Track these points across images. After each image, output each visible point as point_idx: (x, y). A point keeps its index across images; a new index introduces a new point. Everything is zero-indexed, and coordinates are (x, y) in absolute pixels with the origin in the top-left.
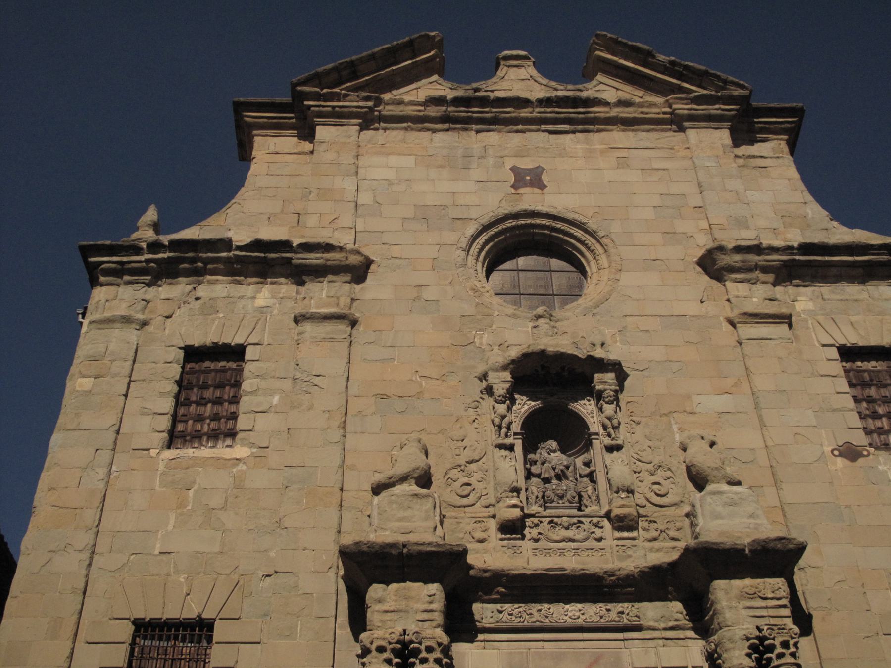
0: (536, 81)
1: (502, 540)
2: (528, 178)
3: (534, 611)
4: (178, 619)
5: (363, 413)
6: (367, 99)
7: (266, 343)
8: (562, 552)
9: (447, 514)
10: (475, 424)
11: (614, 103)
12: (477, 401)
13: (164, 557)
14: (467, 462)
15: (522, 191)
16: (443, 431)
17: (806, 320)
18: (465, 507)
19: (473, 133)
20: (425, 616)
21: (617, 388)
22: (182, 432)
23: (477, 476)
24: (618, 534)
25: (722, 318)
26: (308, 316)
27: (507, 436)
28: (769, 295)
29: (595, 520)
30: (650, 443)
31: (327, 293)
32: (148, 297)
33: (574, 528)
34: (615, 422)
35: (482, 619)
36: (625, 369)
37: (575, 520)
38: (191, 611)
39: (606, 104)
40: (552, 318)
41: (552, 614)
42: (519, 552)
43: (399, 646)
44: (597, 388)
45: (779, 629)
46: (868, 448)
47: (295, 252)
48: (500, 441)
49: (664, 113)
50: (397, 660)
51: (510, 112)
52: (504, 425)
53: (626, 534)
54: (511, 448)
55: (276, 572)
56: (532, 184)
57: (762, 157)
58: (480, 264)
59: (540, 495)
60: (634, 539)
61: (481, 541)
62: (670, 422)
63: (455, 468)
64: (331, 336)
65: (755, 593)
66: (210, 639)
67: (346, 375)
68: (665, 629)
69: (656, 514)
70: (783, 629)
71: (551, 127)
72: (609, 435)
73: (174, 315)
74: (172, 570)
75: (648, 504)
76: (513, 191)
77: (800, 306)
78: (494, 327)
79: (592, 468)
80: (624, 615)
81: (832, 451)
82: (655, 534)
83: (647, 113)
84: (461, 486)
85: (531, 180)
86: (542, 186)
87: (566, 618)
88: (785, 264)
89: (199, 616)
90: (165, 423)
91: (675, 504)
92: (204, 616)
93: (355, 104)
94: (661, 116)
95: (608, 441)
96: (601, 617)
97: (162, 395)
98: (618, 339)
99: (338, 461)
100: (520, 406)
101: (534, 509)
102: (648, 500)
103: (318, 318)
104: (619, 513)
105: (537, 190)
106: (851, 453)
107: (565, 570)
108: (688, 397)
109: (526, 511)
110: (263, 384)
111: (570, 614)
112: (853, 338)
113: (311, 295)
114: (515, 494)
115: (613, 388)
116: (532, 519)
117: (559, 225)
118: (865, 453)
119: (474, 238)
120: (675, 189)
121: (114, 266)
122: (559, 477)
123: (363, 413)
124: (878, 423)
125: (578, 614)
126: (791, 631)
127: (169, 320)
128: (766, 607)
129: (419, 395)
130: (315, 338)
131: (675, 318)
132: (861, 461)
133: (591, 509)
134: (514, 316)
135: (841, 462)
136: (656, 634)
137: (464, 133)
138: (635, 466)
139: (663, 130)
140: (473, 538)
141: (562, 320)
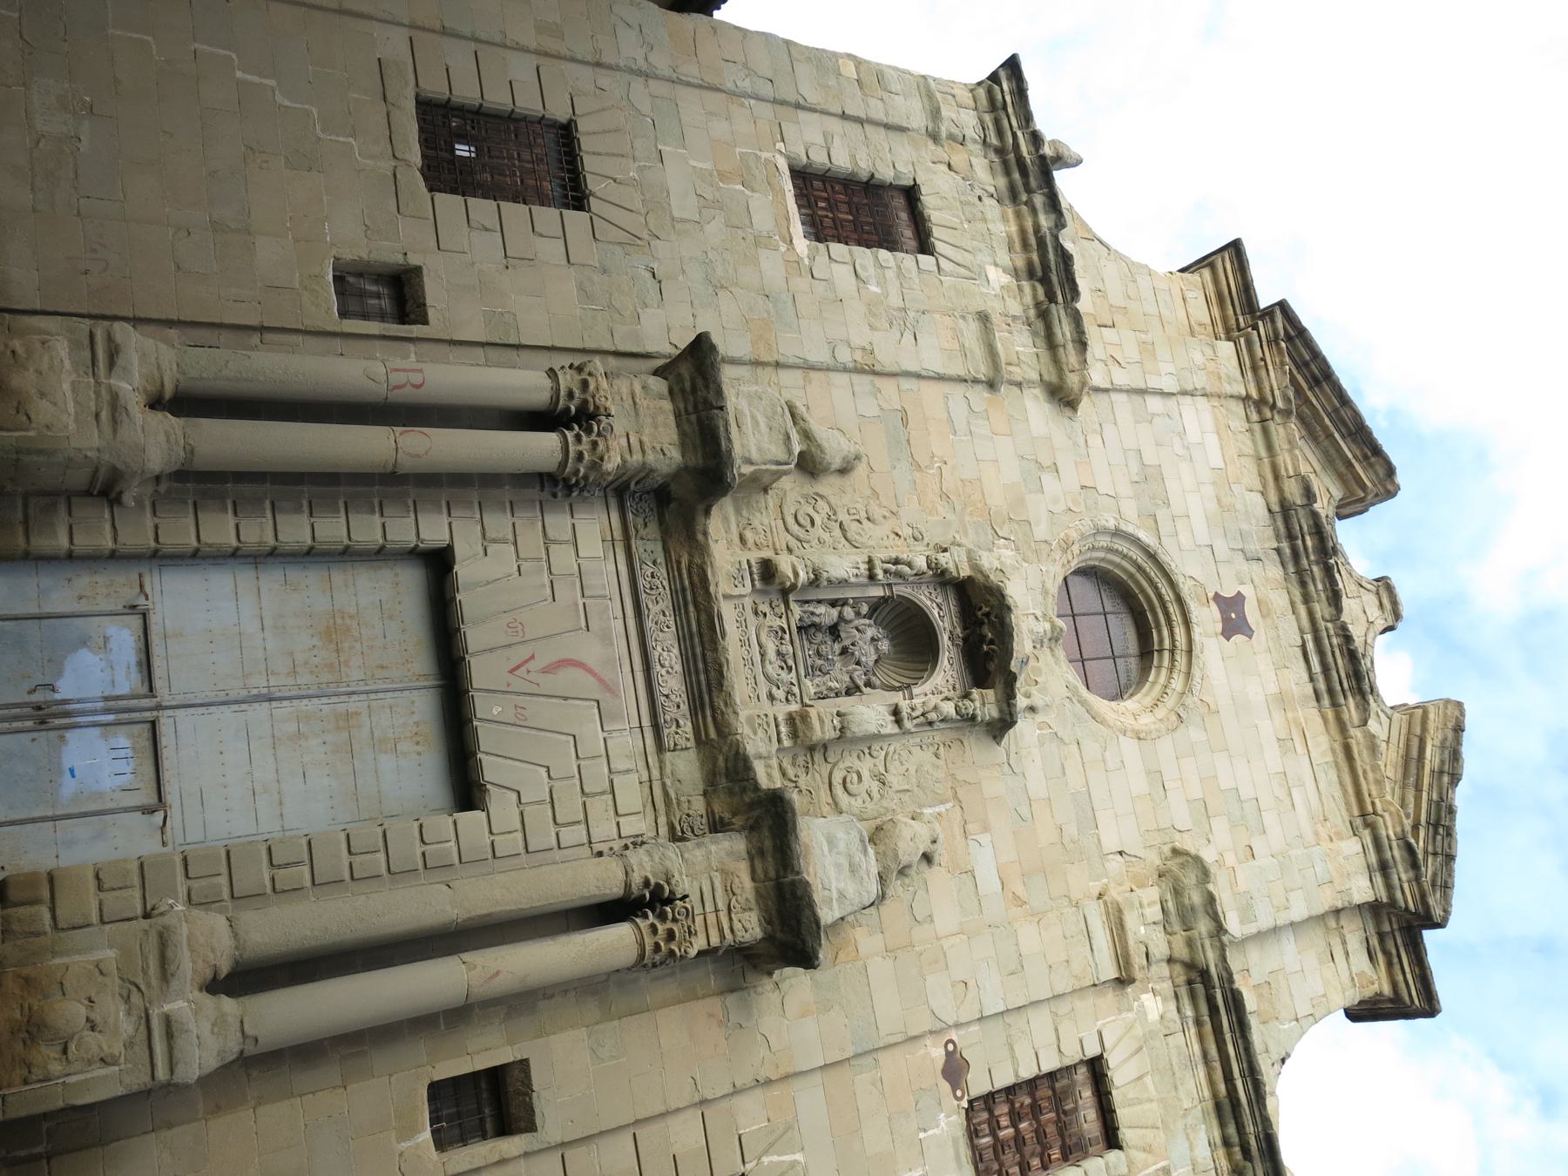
0: (1368, 629)
2: (1233, 616)
3: (662, 605)
4: (583, 169)
5: (879, 395)
6: (1286, 399)
7: (943, 278)
8: (747, 643)
9: (769, 497)
10: (892, 536)
11: (1369, 732)
13: (655, 155)
14: (841, 524)
15: (1214, 607)
16: (875, 494)
17: (1130, 1009)
18: (783, 519)
19: (1275, 545)
21: (979, 719)
23: (825, 536)
24: (781, 718)
25: (1105, 881)
26: (988, 325)
27: (886, 571)
29: (796, 690)
30: (912, 771)
32: (968, 142)
33: (779, 663)
34: (933, 716)
35: (642, 539)
36: (1006, 736)
37: (791, 662)
38: (593, 184)
39: (1364, 723)
40: (1053, 641)
41: (662, 631)
42: (737, 583)
43: (592, 408)
44: (973, 690)
45: (689, 927)
46: (966, 1098)
48: (878, 563)
49: (1373, 804)
50: (573, 408)
51: (1318, 587)
52: (899, 567)
53: (783, 729)
54: (872, 577)
55: (660, 282)
56: (1226, 620)
57: (1347, 954)
58: (1101, 554)
59: (817, 620)
60: (779, 741)
61: (742, 539)
62: (947, 801)
63: (831, 507)
64: (968, 355)
65: (734, 894)
66: (567, 206)
67: (924, 373)
68: (664, 785)
69: (817, 776)
70: (690, 933)
71: (1310, 646)
72: (913, 709)
74: (642, 164)
75: (829, 766)
76: (1211, 595)
77: (1147, 999)
78: (1025, 565)
79: (864, 689)
80: (674, 727)
81: (951, 1041)
82: (791, 772)
83: (1365, 778)
87: (659, 649)
88: (1204, 974)
89: (591, 194)
90: (819, 158)
91: (836, 804)
92: (591, 199)
94: (1368, 800)
95: (904, 705)
96: (667, 696)
97: (853, 157)
98: (1044, 732)
99: (813, 358)
100: (928, 594)
101: (797, 610)
102: (835, 765)
103: (988, 338)
104: (811, 715)
105: (1219, 627)
106: (954, 1069)
107: (723, 638)
108: (986, 829)
109: (791, 597)
110: (890, 274)
112: (1120, 1075)
113: (1015, 333)
114: (812, 576)
115: (978, 712)
116: (782, 606)
117: (1181, 659)
118: (959, 1093)
119: (1135, 541)
120: (1269, 819)
121: (999, 97)
122: (844, 651)
123: (879, 395)
124: (1004, 1121)
125: (667, 663)
126: (688, 944)
128: (717, 911)
130: (962, 335)
131: (1090, 813)
132: (945, 1086)
133: (810, 687)
134: (1045, 592)
135: (938, 1054)
136: (656, 773)
137: (1270, 532)
138: (878, 748)
139: (1347, 804)
140: (744, 529)
141: (1053, 655)
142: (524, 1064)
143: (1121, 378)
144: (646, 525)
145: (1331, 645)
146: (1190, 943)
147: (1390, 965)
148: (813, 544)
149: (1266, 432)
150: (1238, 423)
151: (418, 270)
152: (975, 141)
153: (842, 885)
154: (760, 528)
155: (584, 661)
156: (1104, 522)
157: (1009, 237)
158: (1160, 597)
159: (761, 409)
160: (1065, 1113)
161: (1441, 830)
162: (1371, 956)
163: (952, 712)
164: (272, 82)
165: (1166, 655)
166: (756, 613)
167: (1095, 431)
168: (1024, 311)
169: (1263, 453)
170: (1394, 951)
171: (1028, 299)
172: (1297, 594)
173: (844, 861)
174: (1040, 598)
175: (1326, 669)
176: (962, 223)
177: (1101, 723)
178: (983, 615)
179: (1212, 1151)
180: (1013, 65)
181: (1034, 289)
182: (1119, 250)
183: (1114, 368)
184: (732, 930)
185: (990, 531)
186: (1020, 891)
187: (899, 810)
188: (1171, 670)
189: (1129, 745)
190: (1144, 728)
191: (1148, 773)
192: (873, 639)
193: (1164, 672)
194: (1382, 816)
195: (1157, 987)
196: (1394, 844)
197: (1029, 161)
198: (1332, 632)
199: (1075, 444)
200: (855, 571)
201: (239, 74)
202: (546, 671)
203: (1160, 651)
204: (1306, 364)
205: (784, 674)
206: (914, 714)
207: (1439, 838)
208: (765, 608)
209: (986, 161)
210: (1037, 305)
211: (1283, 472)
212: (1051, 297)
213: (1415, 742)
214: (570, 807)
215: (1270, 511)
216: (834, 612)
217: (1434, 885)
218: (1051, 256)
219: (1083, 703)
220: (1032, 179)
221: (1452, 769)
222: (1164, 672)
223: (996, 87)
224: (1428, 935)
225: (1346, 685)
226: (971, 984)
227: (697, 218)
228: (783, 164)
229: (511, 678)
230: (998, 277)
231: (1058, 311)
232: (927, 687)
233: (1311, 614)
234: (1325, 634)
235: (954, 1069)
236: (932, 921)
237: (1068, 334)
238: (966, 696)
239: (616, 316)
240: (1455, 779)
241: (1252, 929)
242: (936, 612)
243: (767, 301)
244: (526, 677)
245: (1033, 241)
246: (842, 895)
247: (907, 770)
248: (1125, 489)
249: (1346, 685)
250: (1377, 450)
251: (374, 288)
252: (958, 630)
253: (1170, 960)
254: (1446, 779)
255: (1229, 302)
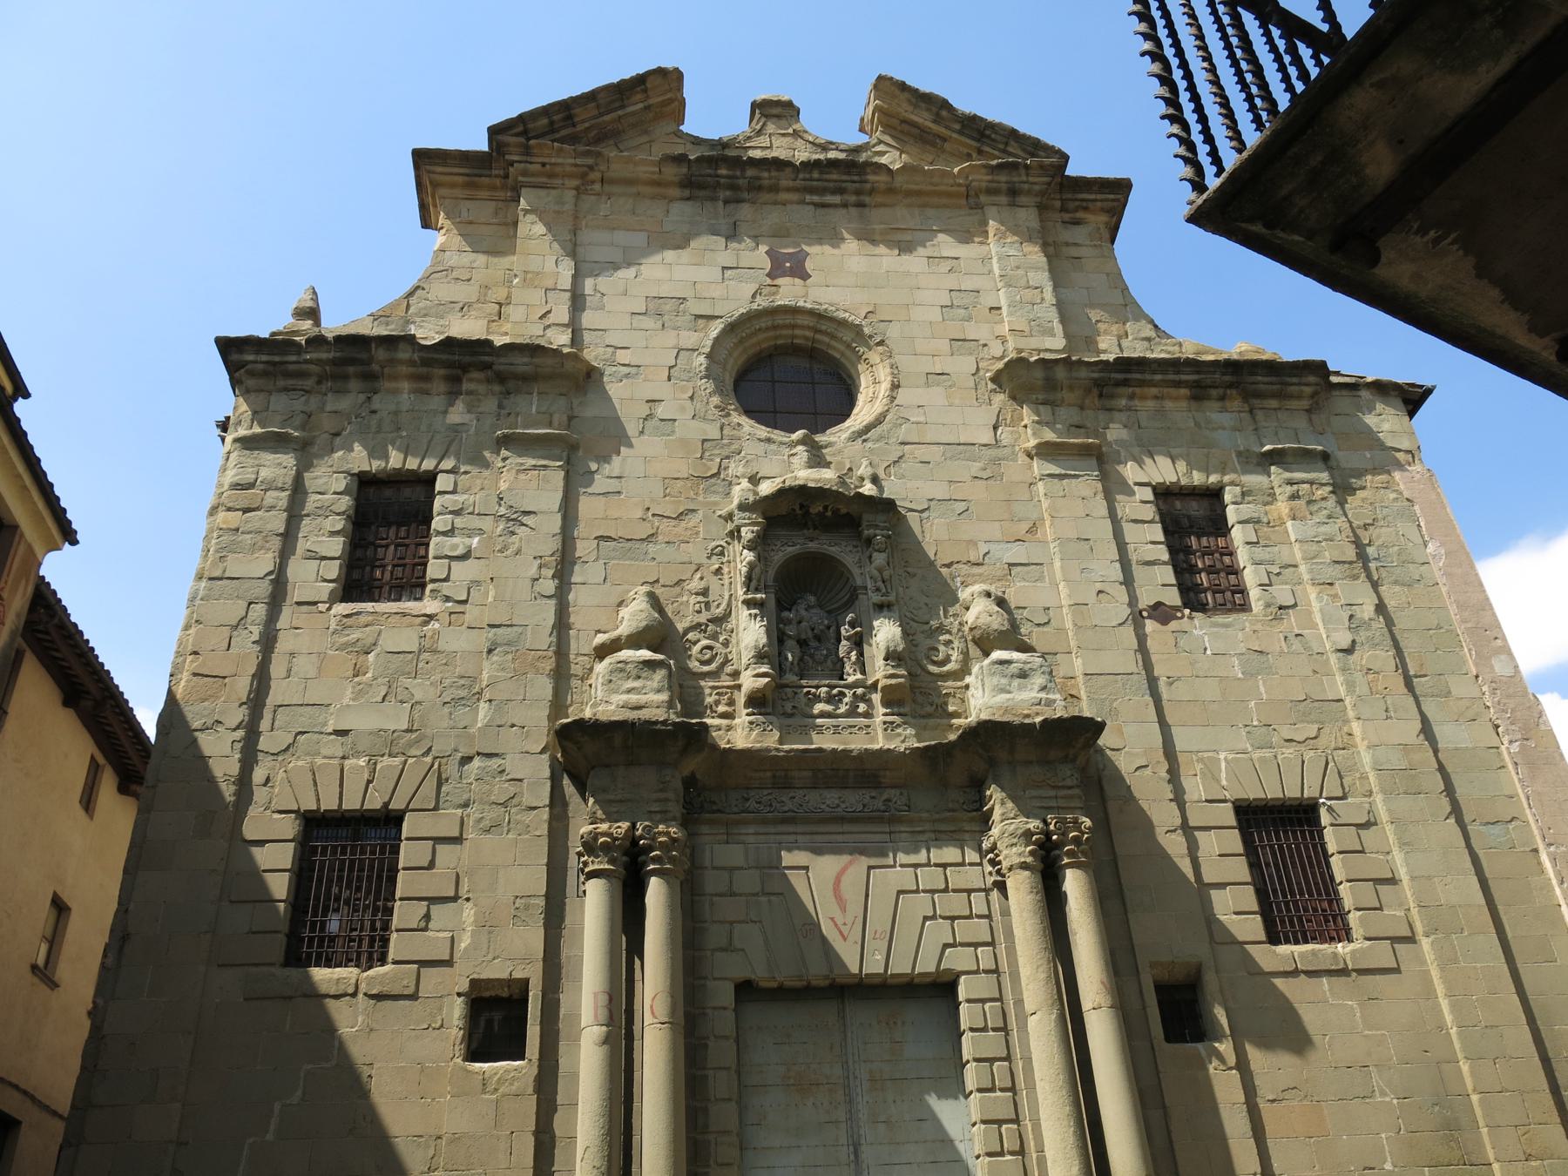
1: (748, 715)
2: (788, 265)
6: (587, 154)
12: (721, 546)
14: (708, 620)
15: (779, 281)
17: (1118, 452)
19: (721, 203)
20: (655, 808)
22: (359, 580)
24: (885, 710)
28: (1076, 419)
29: (860, 691)
31: (538, 406)
38: (375, 802)
44: (866, 532)
47: (498, 356)
57: (1076, 244)
59: (796, 662)
71: (816, 198)
72: (878, 590)
73: (344, 433)
75: (923, 673)
76: (769, 281)
78: (743, 454)
84: (702, 650)
85: (791, 267)
86: (805, 276)
87: (823, 807)
89: (386, 805)
90: (333, 570)
93: (571, 161)
95: (876, 598)
97: (333, 534)
98: (892, 471)
101: (791, 678)
105: (798, 281)
111: (828, 802)
114: (766, 660)
118: (1179, 615)
120: (968, 284)
122: (818, 638)
125: (837, 802)
127: (338, 439)
129: (650, 538)
132: (1174, 625)
137: (708, 204)
138: (908, 627)
142: (1153, 965)
143: (562, 313)
144: (714, 803)
145: (818, 180)
146: (1071, 388)
147: (1086, 209)
148: (728, 650)
149: (613, 182)
150: (604, 208)
151: (474, 983)
152: (307, 402)
153: (1036, 688)
154: (714, 697)
155: (835, 874)
156: (703, 368)
157: (414, 391)
158: (767, 329)
159: (620, 682)
160: (1191, 527)
161: (987, 132)
162: (1077, 222)
163: (883, 556)
164: (277, 1106)
165: (818, 336)
166: (792, 715)
167: (614, 353)
168: (493, 394)
169: (634, 190)
170: (1077, 203)
171: (482, 388)
172: (765, 197)
173: (1016, 682)
174: (773, 447)
175: (841, 191)
176: (402, 437)
177: (885, 417)
178: (801, 509)
179: (1227, 411)
180: (228, 347)
181: (471, 380)
182: (419, 277)
183: (552, 319)
184: (1070, 788)
185: (713, 480)
186: (1025, 526)
187: (959, 619)
188: (833, 337)
189: (903, 396)
190: (889, 378)
191: (927, 385)
192: (806, 610)
193: (834, 343)
194: (971, 181)
195: (1102, 424)
196: (996, 178)
197: (338, 354)
198: (807, 176)
199: (627, 376)
200: (759, 619)
201: (269, 1137)
202: (843, 910)
203: (814, 341)
204: (552, 123)
205: (846, 700)
206: (884, 590)
207: (993, 136)
208: (788, 707)
209: (329, 395)
210: (488, 381)
211: (656, 177)
212: (488, 366)
213: (906, 127)
214: (956, 904)
215: (688, 199)
216: (791, 643)
217: (1033, 155)
218: (444, 357)
219: (868, 428)
220: (359, 356)
221: (937, 105)
222: (834, 343)
223: (249, 367)
224: (1071, 171)
225: (856, 178)
226: (1099, 586)
227: (407, 706)
228: (342, 608)
229: (851, 939)
230: (457, 414)
231: (500, 364)
232: (856, 571)
233: (788, 190)
234: (809, 183)
235: (1161, 613)
236: (1048, 609)
237: (526, 360)
238: (869, 541)
239: (514, 801)
240: (945, 104)
241: (1058, 328)
242: (791, 549)
243: (496, 652)
244: (848, 927)
245: (423, 370)
246: (1043, 688)
247: (926, 604)
248: (670, 339)
249: (856, 178)
250: (640, 81)
251: (482, 1024)
252: (805, 531)
253: (1082, 408)
254: (944, 113)
255: (476, 179)
